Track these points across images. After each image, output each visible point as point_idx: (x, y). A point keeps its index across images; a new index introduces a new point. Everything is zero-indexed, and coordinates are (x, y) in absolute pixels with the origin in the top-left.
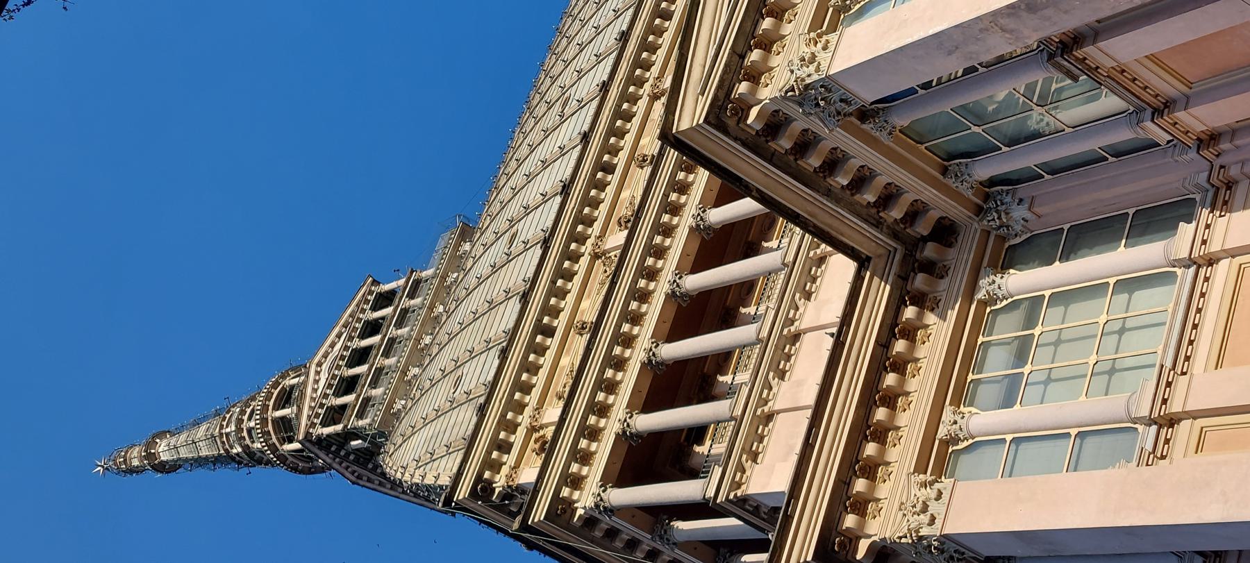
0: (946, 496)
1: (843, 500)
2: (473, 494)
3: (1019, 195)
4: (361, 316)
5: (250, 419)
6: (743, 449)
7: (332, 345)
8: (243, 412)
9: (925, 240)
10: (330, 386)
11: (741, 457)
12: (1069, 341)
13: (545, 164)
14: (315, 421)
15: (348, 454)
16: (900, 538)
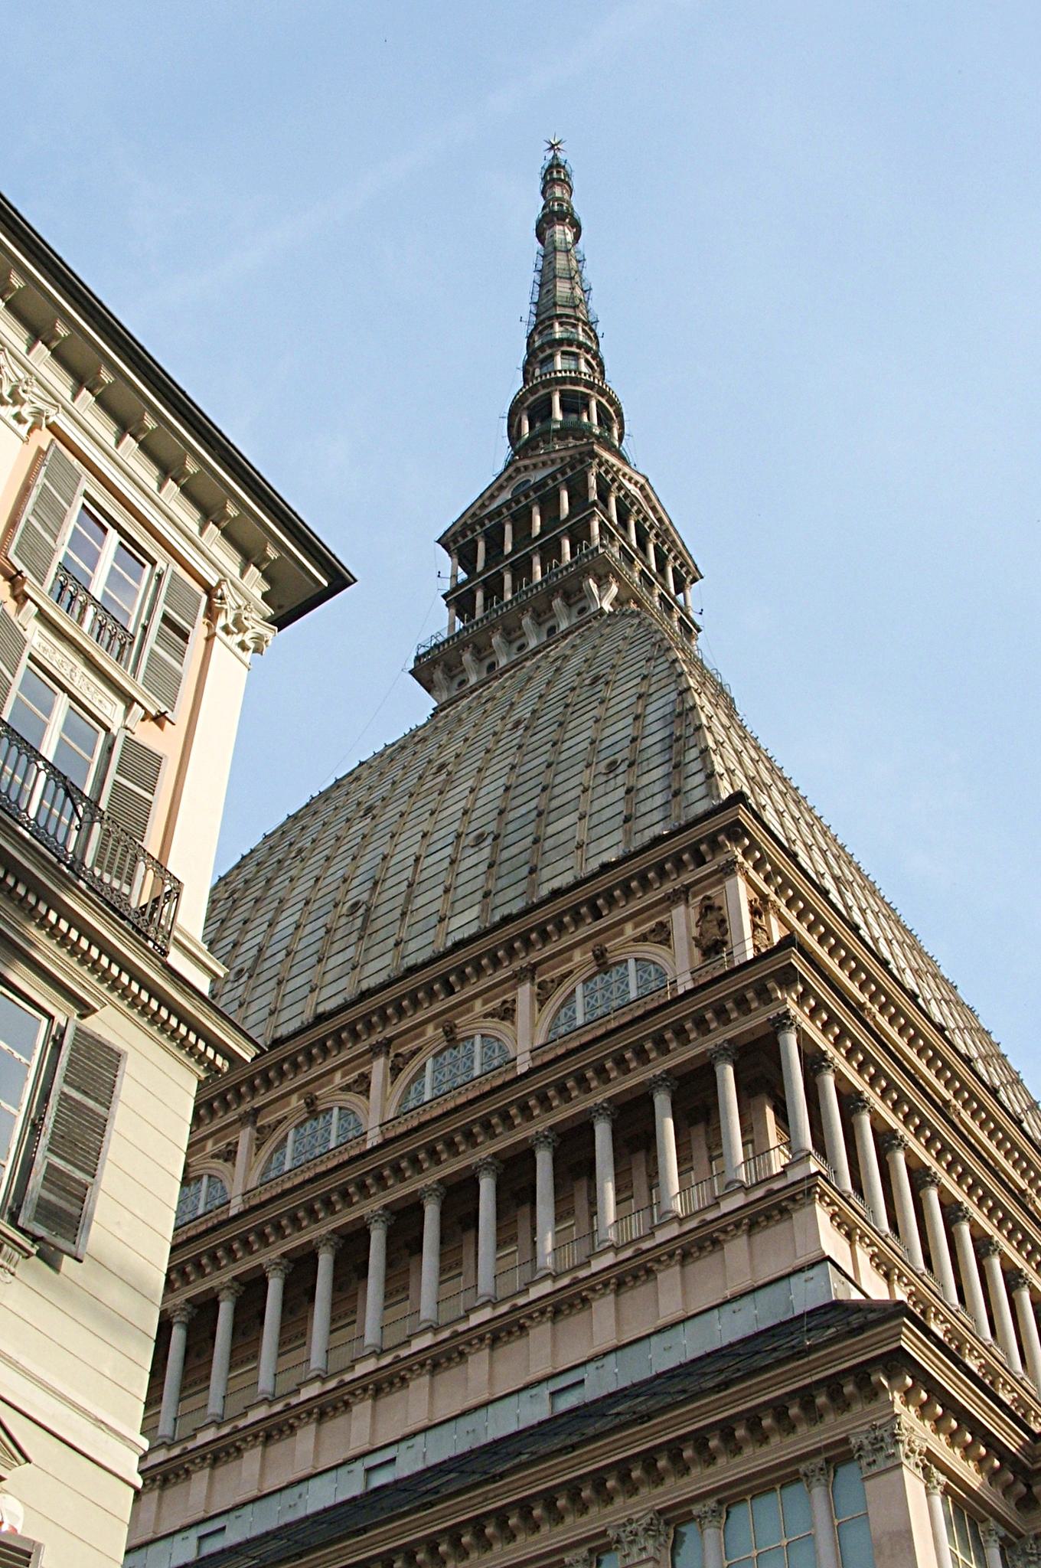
2: (738, 823)
4: (673, 554)
5: (588, 362)
6: (841, 1209)
7: (654, 509)
9: (1029, 1487)
10: (626, 496)
11: (838, 1205)
14: (603, 468)
16: (899, 1424)
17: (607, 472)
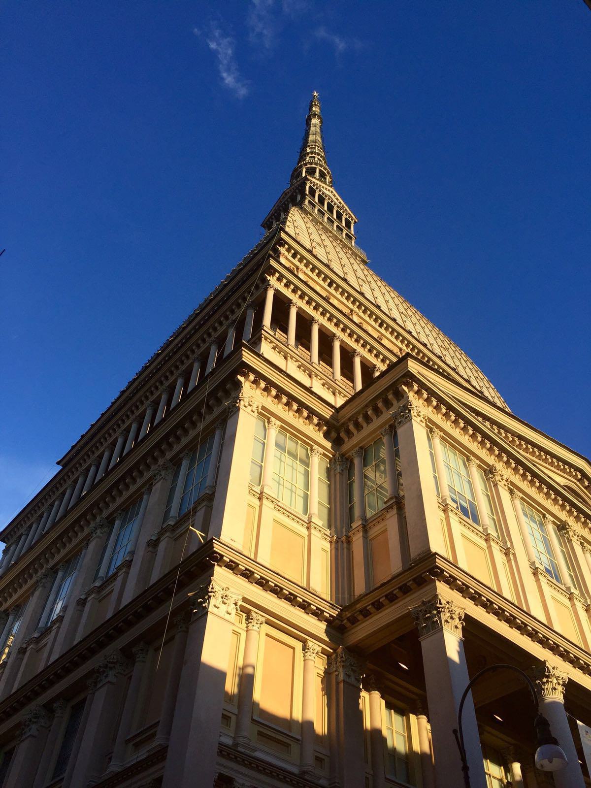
0: (252, 413)
1: (259, 376)
3: (345, 471)
5: (318, 159)
7: (337, 199)
8: (321, 157)
9: (339, 434)
10: (323, 194)
11: (275, 343)
12: (292, 472)
13: (387, 302)
14: (312, 184)
15: (296, 193)
16: (242, 393)
17: (314, 186)
